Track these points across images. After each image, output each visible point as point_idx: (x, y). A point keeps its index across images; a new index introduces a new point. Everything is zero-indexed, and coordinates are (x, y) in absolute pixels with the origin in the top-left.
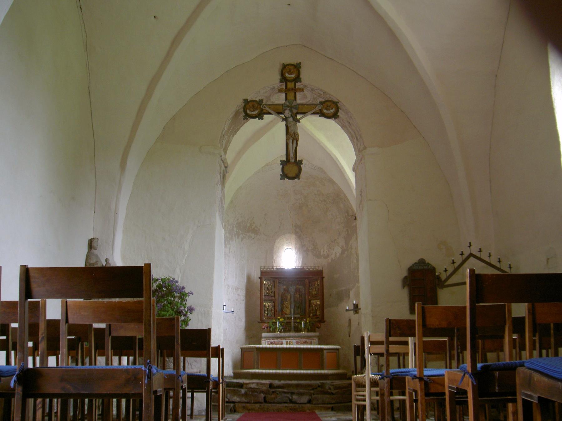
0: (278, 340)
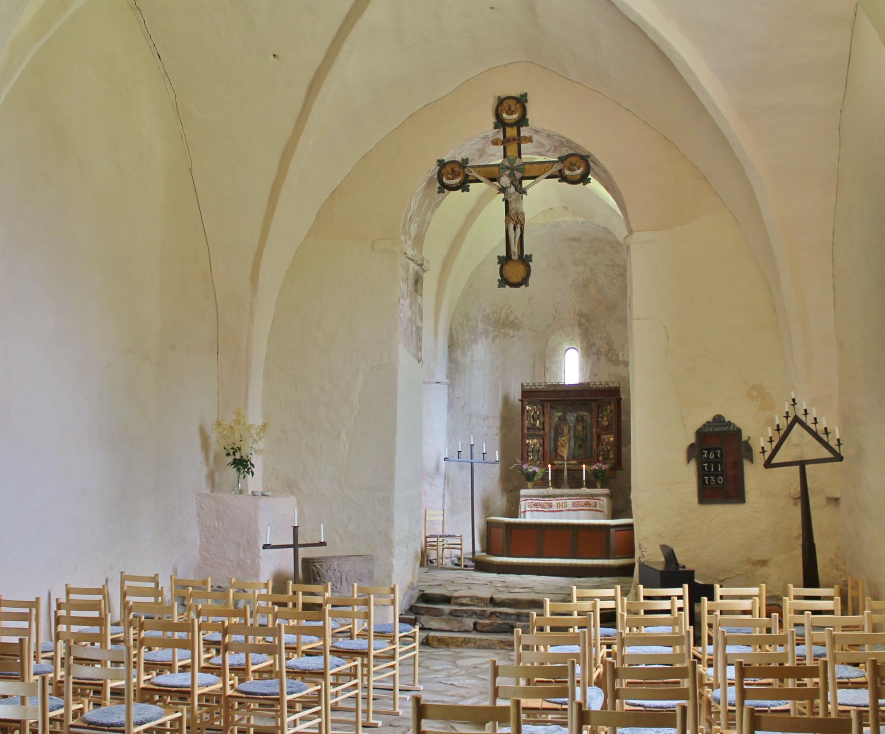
0: (545, 500)
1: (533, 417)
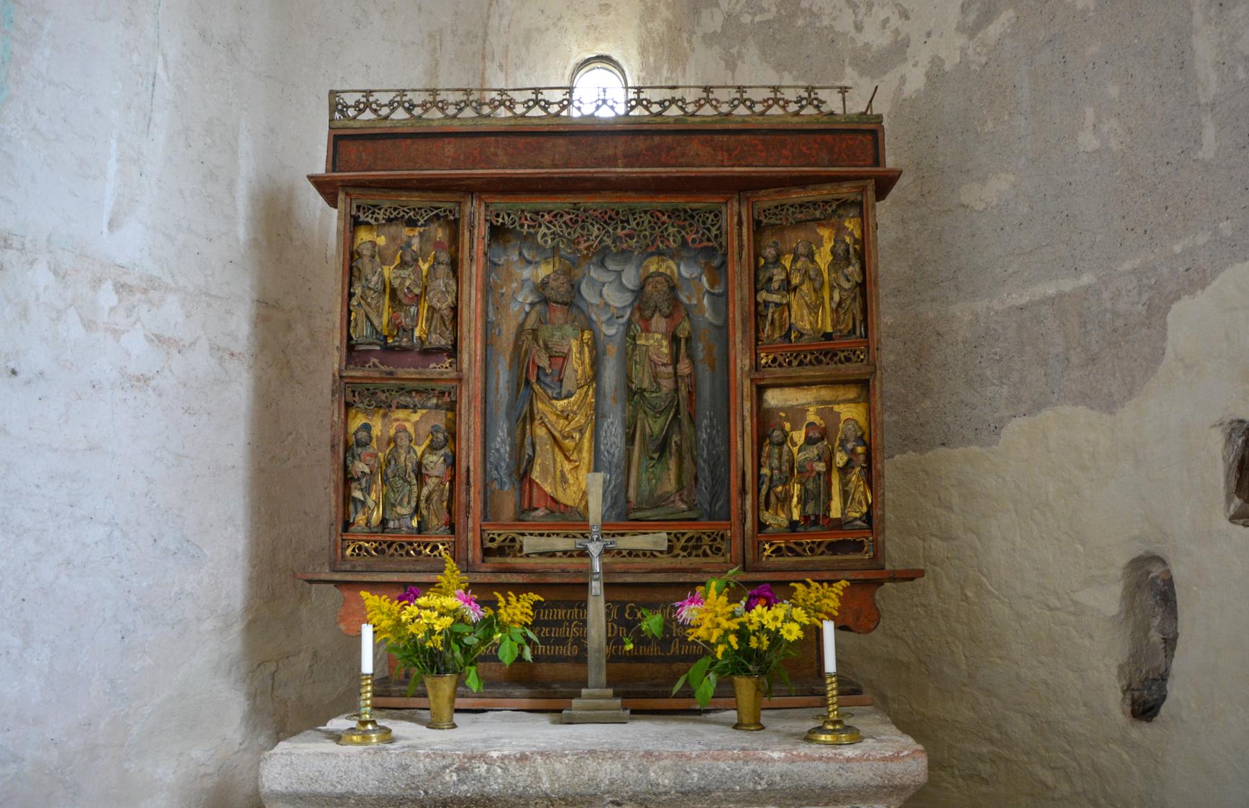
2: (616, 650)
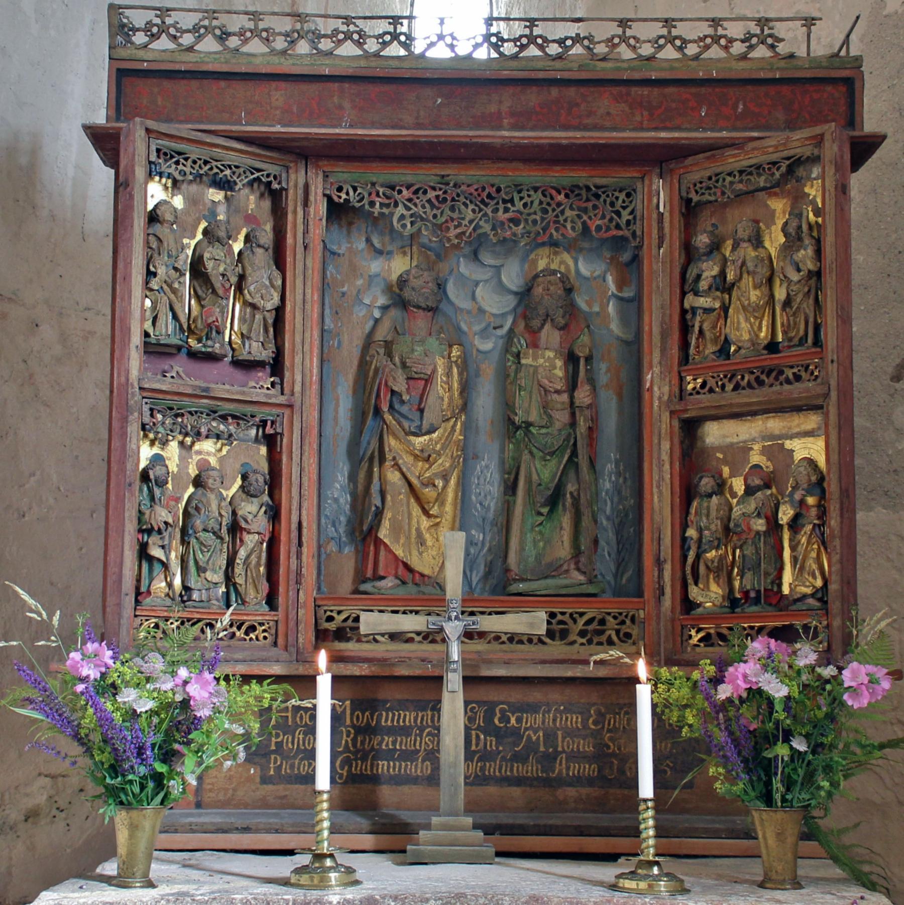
1: (197, 269)
2: (482, 769)
